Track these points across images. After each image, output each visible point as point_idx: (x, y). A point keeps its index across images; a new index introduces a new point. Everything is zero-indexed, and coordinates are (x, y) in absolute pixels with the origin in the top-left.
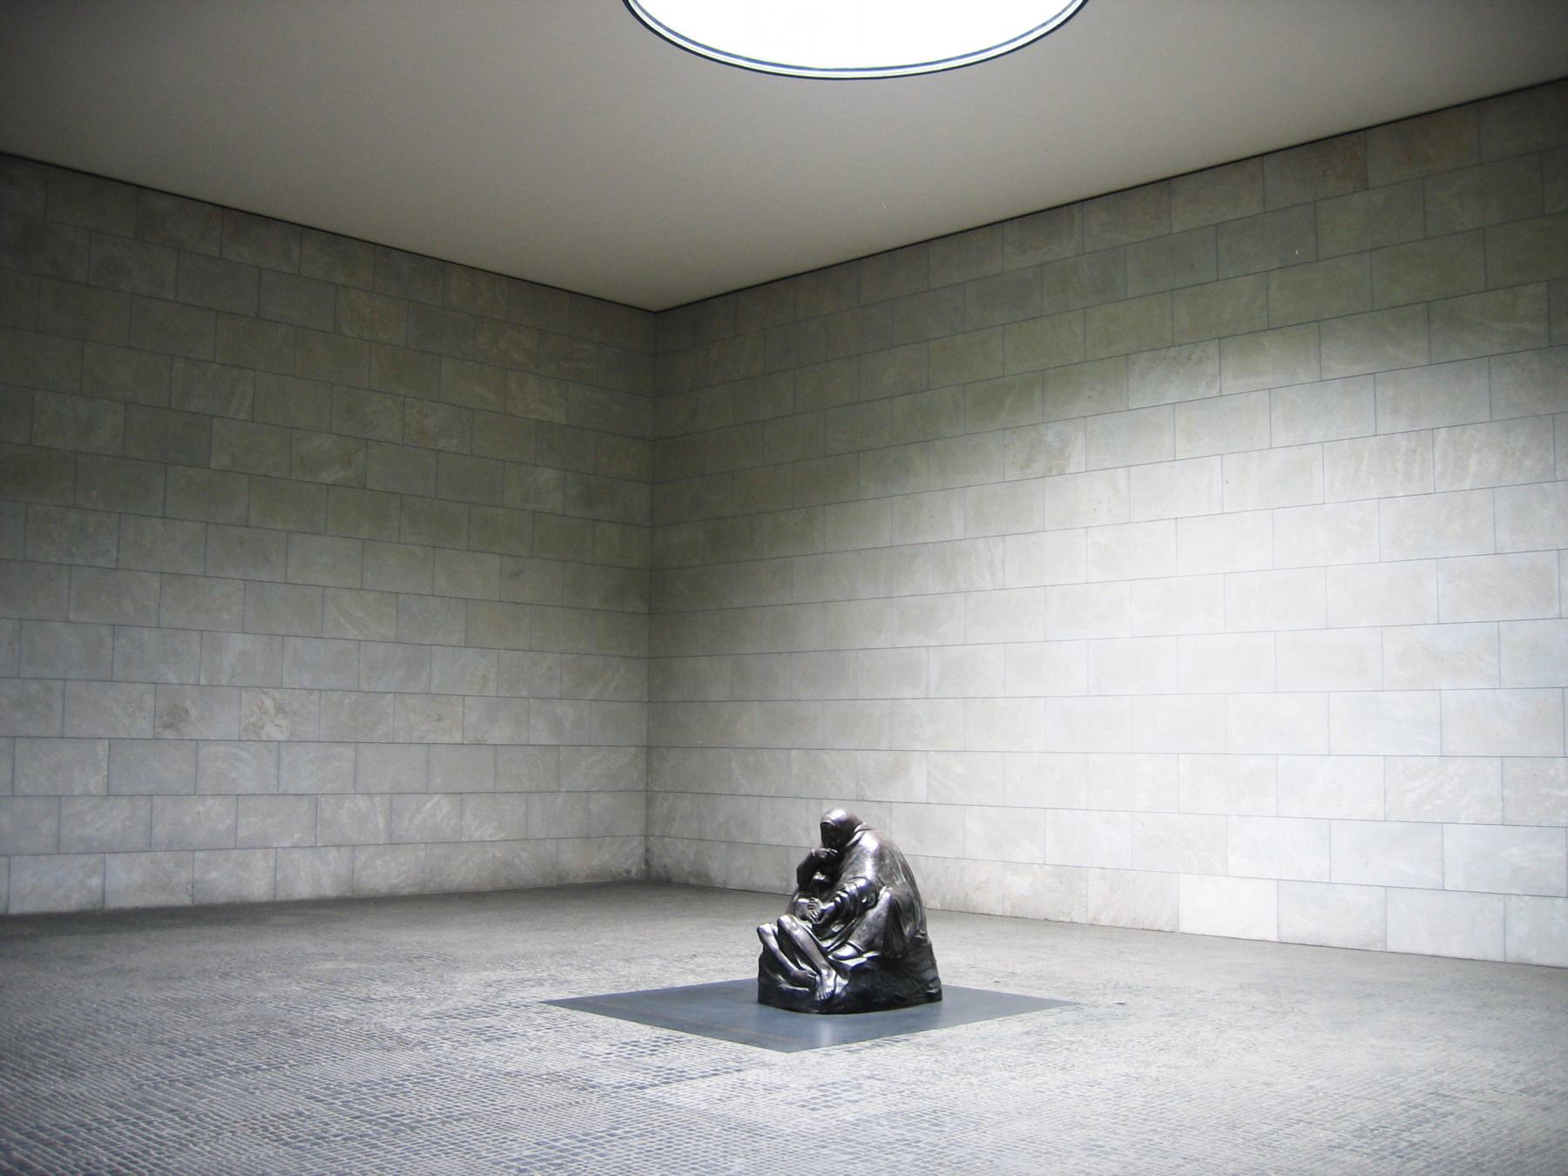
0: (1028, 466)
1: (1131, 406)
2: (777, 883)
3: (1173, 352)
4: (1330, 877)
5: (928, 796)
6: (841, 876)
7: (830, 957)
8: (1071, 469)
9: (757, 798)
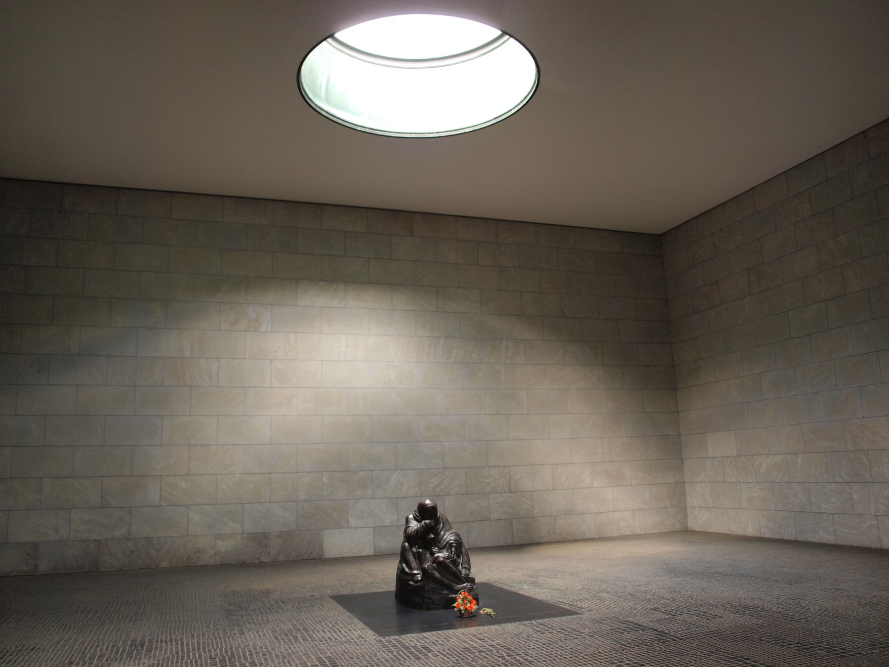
0: (235, 324)
1: (298, 303)
2: (25, 568)
3: (321, 283)
4: (398, 523)
5: (160, 501)
6: (439, 534)
7: (463, 576)
8: (263, 329)
9: (7, 512)
